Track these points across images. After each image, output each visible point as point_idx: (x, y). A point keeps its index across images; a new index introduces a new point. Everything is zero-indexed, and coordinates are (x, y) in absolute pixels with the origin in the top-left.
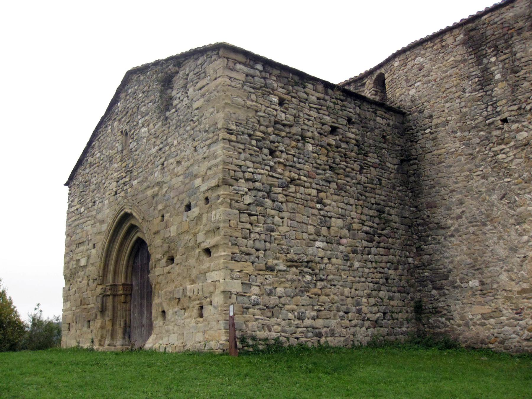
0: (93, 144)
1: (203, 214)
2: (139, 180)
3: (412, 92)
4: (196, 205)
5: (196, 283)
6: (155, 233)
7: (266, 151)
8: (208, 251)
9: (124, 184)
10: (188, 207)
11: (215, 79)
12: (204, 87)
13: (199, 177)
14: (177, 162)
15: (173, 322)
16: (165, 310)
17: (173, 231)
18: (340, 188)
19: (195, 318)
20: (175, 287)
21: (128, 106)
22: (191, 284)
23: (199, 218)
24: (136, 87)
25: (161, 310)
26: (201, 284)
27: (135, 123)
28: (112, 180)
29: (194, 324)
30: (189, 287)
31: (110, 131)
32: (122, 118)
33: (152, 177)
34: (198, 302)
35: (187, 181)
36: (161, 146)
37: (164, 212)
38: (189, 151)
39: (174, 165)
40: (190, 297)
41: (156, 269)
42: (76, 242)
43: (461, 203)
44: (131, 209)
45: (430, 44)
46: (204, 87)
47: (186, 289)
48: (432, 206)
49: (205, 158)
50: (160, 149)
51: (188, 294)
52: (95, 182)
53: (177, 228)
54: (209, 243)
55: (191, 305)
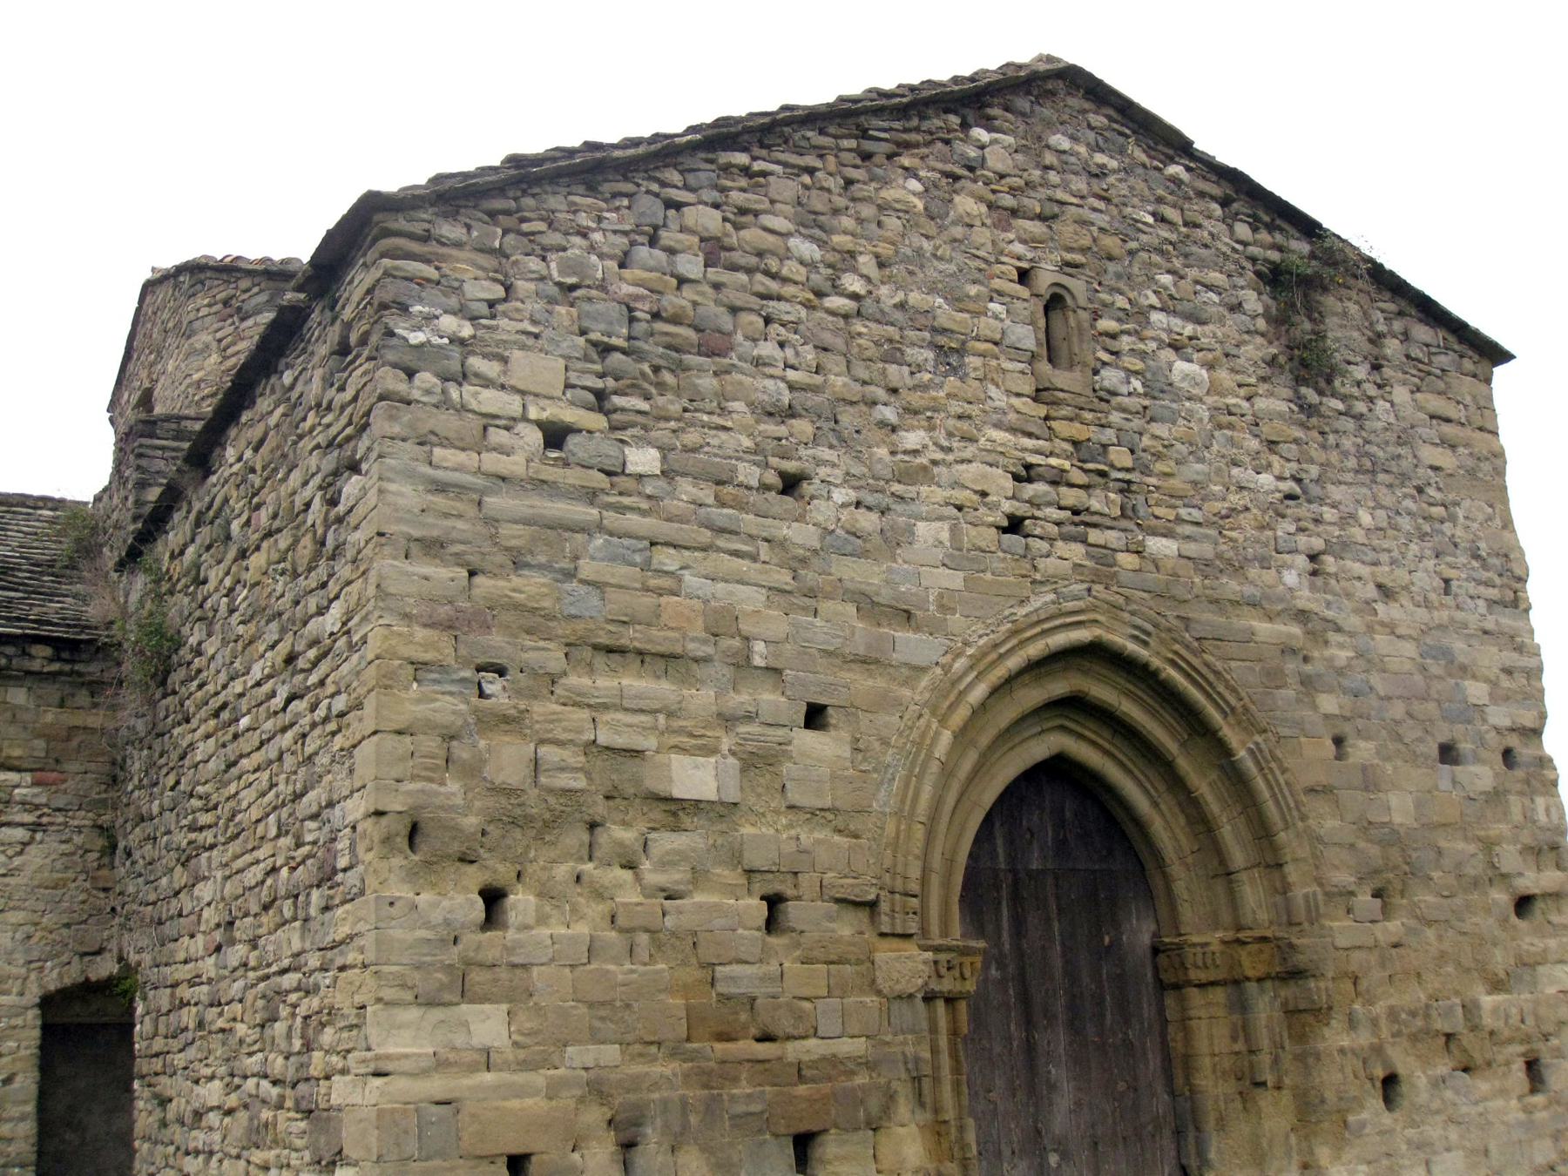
0: (741, 158)
1: (1507, 792)
2: (1192, 549)
4: (1478, 760)
5: (1508, 991)
6: (1311, 790)
8: (1523, 904)
9: (1076, 512)
10: (1448, 753)
11: (1481, 429)
12: (1448, 420)
13: (1474, 677)
14: (1380, 586)
15: (1438, 1112)
16: (1401, 1071)
17: (1399, 808)
19: (1520, 1098)
20: (1430, 997)
21: (1060, 195)
22: (1489, 993)
23: (1496, 796)
24: (1100, 158)
25: (1380, 1073)
26: (1528, 996)
27: (1121, 302)
28: (970, 450)
29: (1522, 1116)
30: (1488, 1001)
31: (920, 205)
32: (1014, 213)
33: (1269, 576)
34: (1521, 1049)
35: (1436, 668)
36: (1298, 490)
37: (1347, 729)
38: (1424, 580)
39: (1371, 592)
40: (1492, 1033)
41: (1328, 923)
42: (562, 629)
44: (1145, 644)
46: (1448, 420)
47: (1476, 1005)
49: (1486, 632)
50: (1290, 497)
51: (1488, 1021)
52: (791, 375)
53: (1419, 805)
54: (1531, 881)
55: (1500, 1058)
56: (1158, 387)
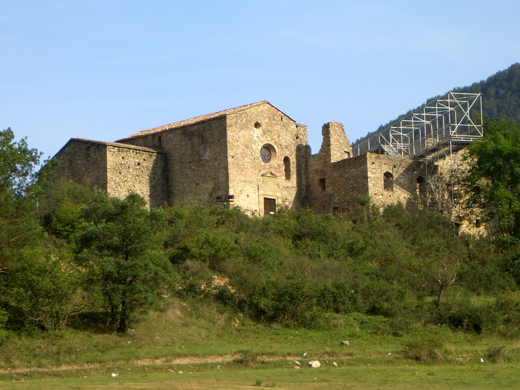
3: (168, 146)
7: (118, 173)
18: (140, 182)
43: (178, 186)
45: (173, 131)
48: (171, 186)
56: (77, 164)
